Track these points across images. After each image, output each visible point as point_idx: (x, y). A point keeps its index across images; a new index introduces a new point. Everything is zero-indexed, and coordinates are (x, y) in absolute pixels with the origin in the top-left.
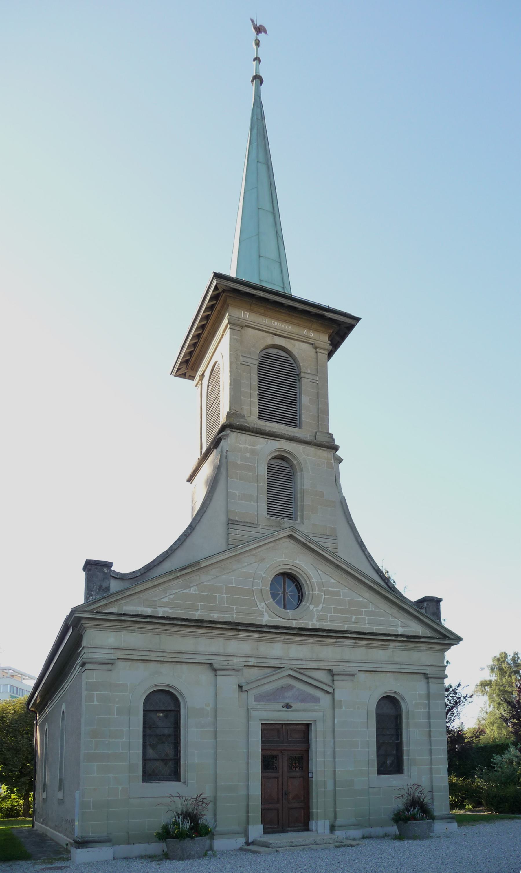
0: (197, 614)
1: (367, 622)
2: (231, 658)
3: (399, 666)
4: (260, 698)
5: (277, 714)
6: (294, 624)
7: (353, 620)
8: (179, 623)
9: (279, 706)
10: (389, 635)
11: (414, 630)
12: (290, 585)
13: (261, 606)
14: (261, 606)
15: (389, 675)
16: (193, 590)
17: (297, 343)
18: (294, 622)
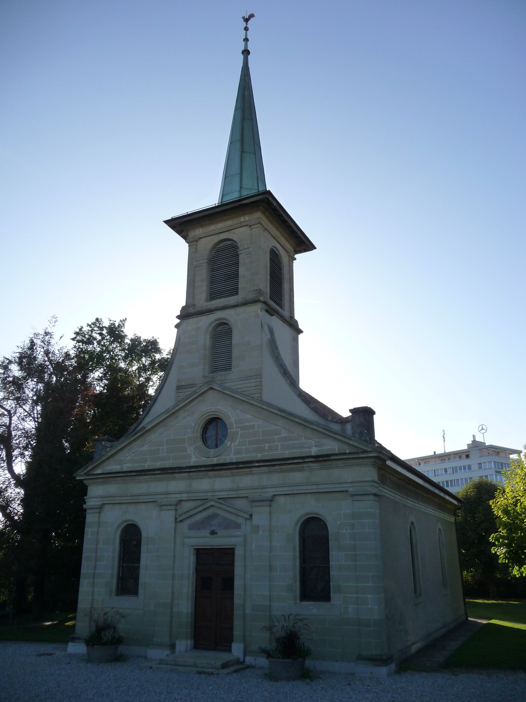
0: (146, 465)
1: (279, 448)
2: (170, 496)
3: (315, 487)
4: (192, 527)
5: (206, 540)
6: (215, 461)
7: (266, 448)
8: (117, 475)
9: (206, 533)
10: (294, 458)
11: (329, 447)
12: (213, 428)
13: (190, 450)
14: (190, 450)
15: (309, 496)
16: (146, 448)
17: (236, 231)
18: (215, 459)
